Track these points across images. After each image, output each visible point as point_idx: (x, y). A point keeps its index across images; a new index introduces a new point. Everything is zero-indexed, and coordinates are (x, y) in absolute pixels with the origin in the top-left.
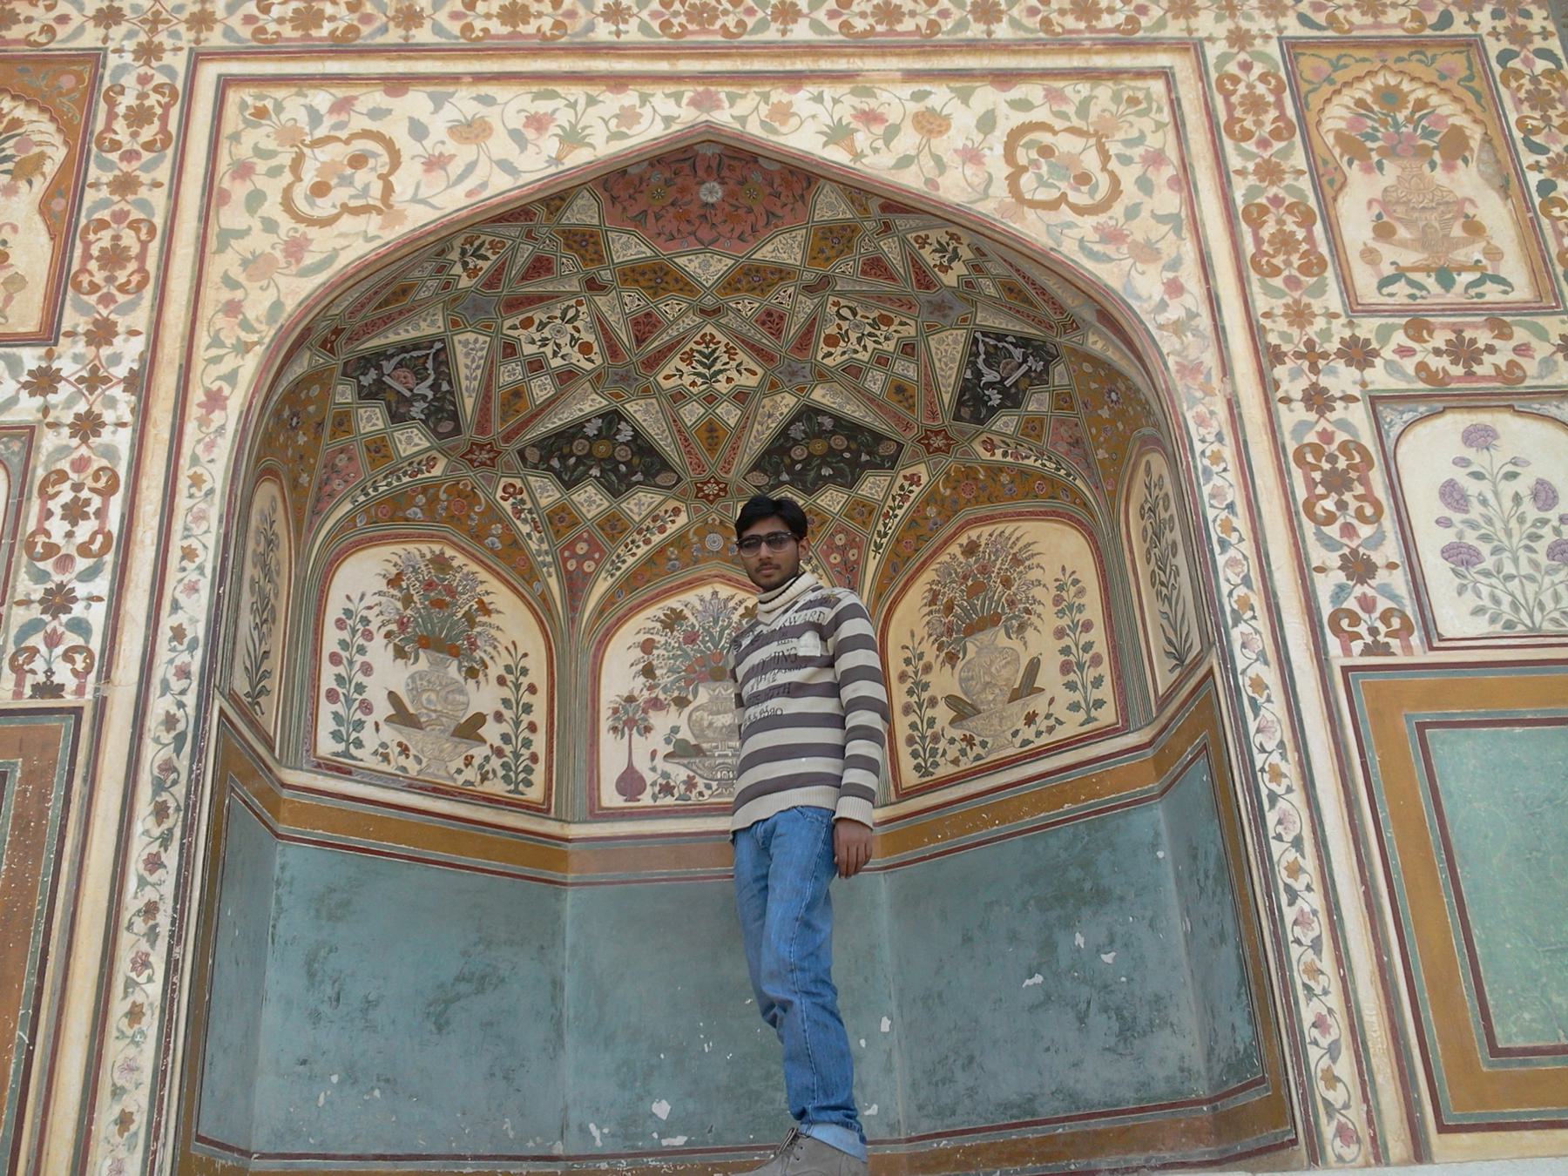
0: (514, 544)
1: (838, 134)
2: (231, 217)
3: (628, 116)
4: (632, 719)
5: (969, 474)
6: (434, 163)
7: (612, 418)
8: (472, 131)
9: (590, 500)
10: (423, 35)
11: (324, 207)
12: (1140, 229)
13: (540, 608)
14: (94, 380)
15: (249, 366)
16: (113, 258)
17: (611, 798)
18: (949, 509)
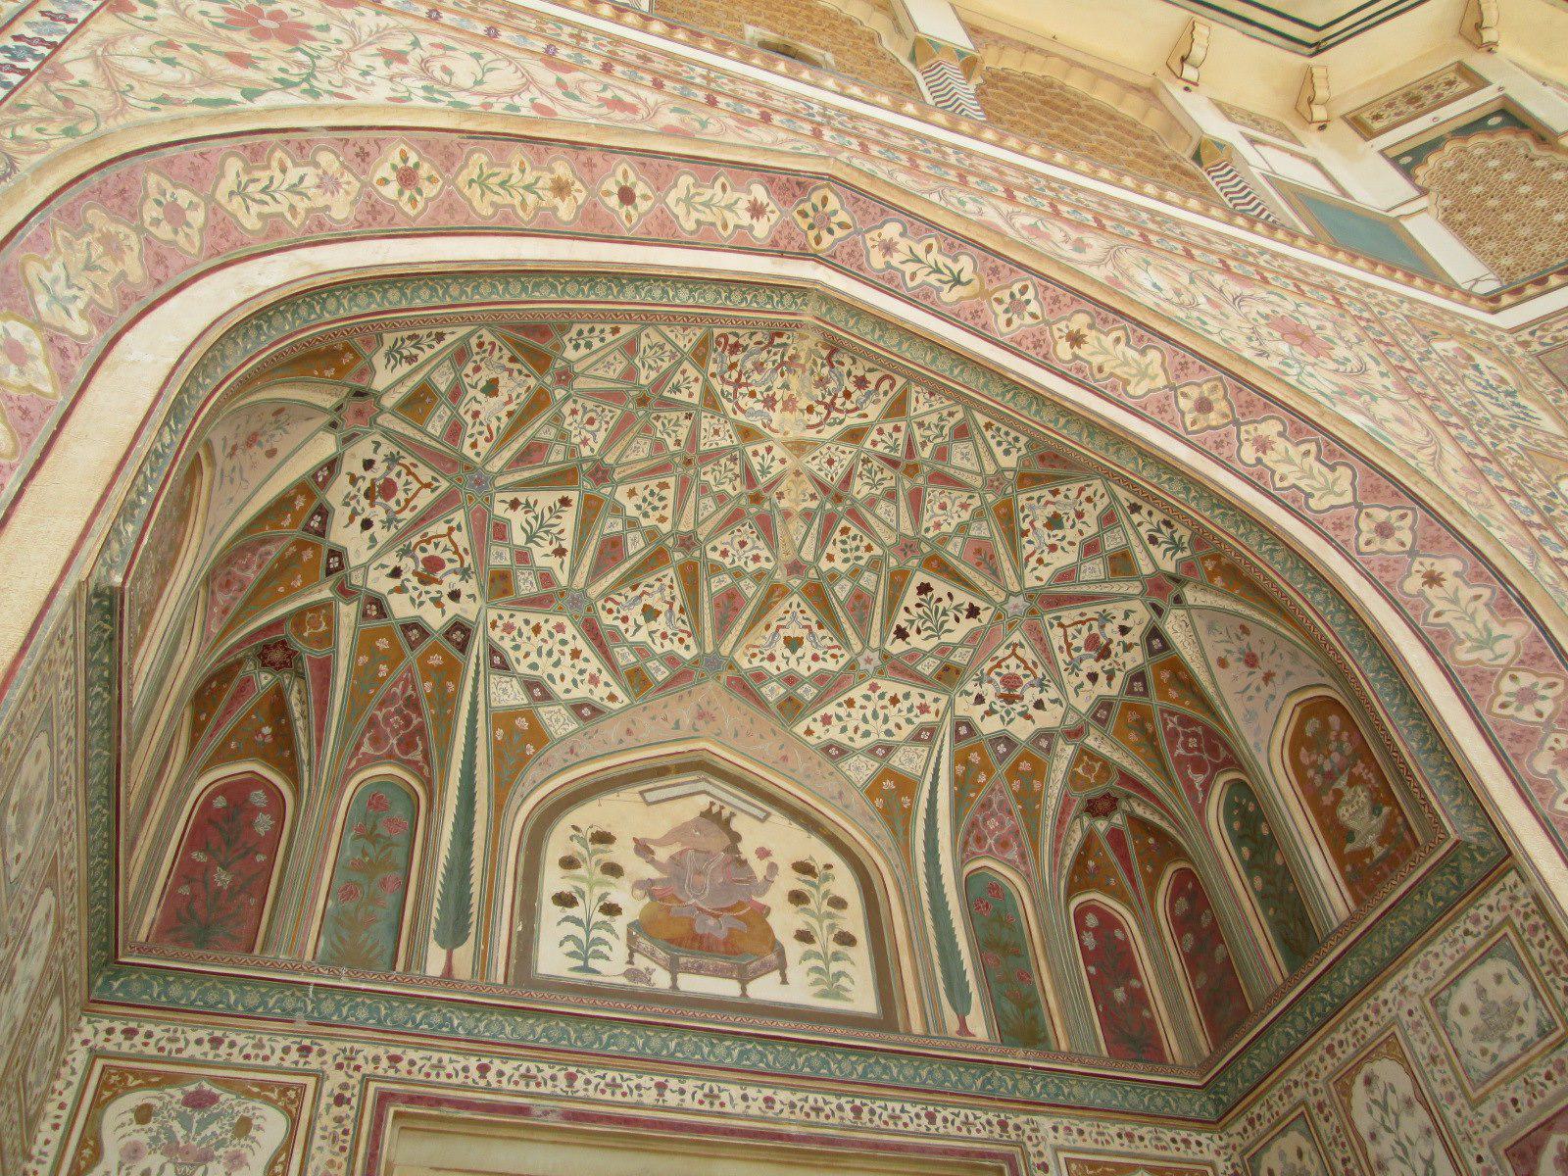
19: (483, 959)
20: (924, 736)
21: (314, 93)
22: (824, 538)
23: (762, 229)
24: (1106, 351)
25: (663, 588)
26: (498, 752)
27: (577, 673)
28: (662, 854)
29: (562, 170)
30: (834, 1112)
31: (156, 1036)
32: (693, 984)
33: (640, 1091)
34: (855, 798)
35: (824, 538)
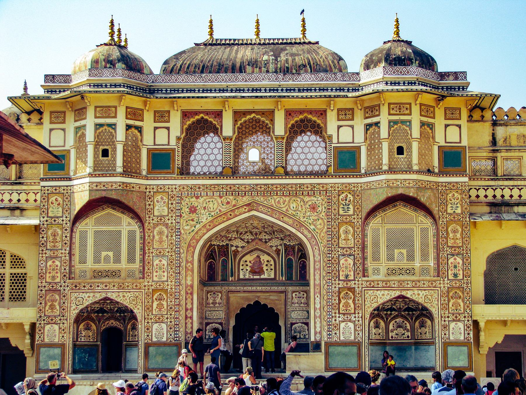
0: (382, 316)
1: (411, 295)
2: (366, 303)
3: (395, 293)
4: (392, 331)
5: (422, 313)
6: (381, 298)
7: (391, 307)
8: (383, 295)
9: (389, 312)
10: (379, 286)
11: (373, 302)
12: (434, 305)
13: (384, 321)
14: (358, 317)
15: (369, 316)
16: (358, 307)
17: (390, 338)
18: (421, 315)
19: (235, 278)
20: (281, 245)
21: (199, 223)
22: (264, 229)
23: (246, 210)
24: (286, 219)
25: (248, 234)
26: (234, 255)
27: (240, 243)
28: (252, 262)
29: (223, 216)
30: (268, 288)
31: (210, 288)
32: (255, 277)
33: (250, 288)
34: (274, 252)
35: (264, 229)
